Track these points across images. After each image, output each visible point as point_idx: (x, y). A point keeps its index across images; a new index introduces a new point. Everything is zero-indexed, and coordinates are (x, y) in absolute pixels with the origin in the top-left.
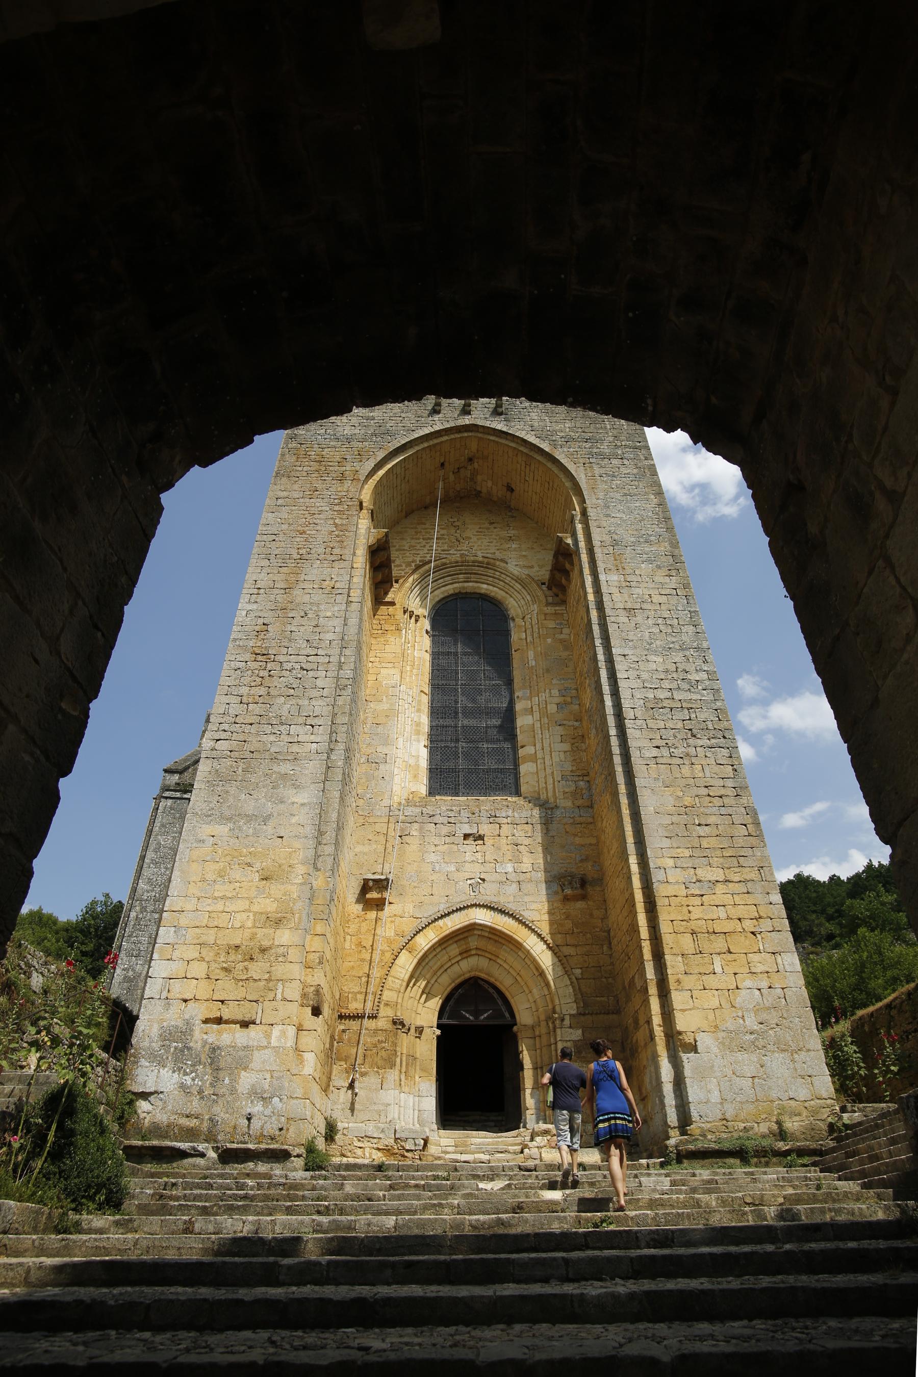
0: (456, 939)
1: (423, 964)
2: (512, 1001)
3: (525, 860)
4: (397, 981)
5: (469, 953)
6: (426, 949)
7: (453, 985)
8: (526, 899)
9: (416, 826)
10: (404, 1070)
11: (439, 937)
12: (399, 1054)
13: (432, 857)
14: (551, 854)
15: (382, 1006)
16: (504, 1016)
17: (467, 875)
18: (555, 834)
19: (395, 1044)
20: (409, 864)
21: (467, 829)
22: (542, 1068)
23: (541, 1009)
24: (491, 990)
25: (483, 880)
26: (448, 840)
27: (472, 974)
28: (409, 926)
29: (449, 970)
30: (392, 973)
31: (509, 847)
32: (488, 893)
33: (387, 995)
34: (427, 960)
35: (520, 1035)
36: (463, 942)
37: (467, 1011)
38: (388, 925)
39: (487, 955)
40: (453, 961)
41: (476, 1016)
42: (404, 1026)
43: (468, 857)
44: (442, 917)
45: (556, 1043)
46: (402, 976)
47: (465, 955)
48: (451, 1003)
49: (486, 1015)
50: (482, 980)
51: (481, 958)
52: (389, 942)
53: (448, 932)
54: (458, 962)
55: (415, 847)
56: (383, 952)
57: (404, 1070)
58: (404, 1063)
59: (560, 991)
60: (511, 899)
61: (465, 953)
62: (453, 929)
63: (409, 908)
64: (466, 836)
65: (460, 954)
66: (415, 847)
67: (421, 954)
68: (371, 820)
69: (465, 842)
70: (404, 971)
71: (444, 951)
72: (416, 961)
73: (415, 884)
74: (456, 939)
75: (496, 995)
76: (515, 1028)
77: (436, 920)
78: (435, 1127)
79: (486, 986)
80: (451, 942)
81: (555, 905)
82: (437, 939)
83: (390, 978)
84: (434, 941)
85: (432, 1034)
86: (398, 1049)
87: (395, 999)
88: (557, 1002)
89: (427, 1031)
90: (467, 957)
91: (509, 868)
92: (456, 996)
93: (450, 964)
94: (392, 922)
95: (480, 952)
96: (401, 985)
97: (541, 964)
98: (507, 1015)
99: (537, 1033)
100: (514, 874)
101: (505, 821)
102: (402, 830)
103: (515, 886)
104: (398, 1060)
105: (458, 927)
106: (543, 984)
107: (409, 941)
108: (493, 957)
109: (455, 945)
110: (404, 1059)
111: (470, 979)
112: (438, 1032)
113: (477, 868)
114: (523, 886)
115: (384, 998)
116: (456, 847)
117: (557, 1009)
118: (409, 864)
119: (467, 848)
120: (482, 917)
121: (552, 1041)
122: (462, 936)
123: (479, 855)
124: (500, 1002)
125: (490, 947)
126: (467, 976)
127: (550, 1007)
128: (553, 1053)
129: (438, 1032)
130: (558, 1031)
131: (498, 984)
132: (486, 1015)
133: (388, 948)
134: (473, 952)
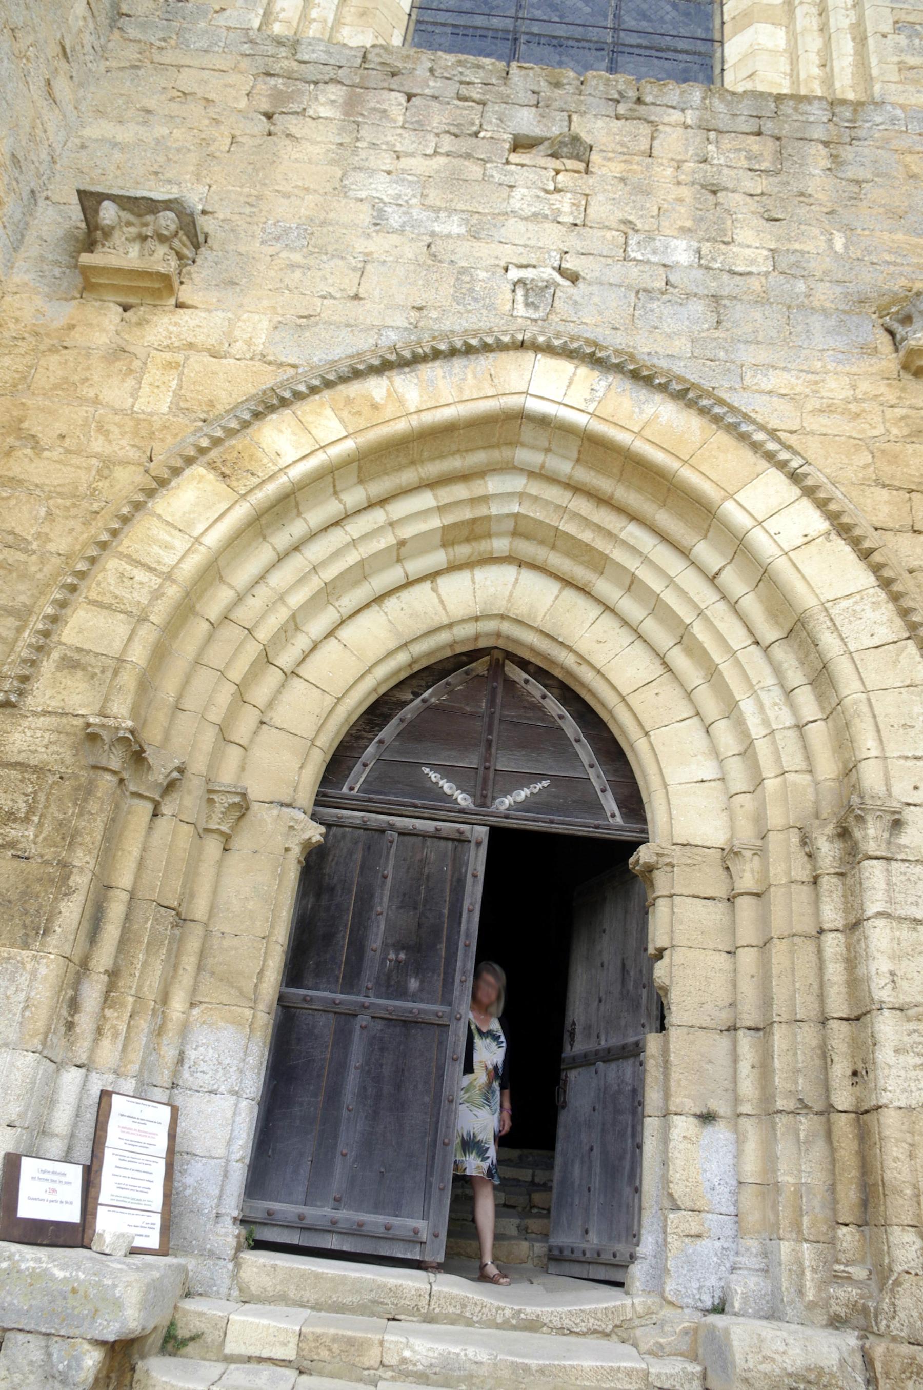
0: (433, 469)
1: (282, 539)
2: (640, 753)
3: (744, 235)
4: (140, 575)
5: (483, 546)
6: (296, 472)
7: (402, 658)
8: (747, 355)
9: (335, 92)
10: (104, 958)
11: (362, 439)
12: (80, 880)
13: (382, 188)
14: (848, 230)
15: (48, 666)
16: (596, 808)
17: (508, 254)
18: (862, 174)
19: (69, 837)
20: (287, 196)
21: (526, 121)
22: (761, 1030)
23: (771, 784)
24: (554, 706)
25: (574, 278)
26: (447, 143)
27: (490, 626)
28: (235, 383)
29: (391, 603)
30: (126, 544)
31: (685, 192)
32: (592, 314)
33: (84, 627)
34: (297, 528)
35: (661, 882)
36: (460, 492)
37: (448, 772)
38: (153, 374)
39: (556, 561)
40: (416, 566)
41: (483, 800)
42: (138, 758)
43: (521, 200)
44: (384, 367)
45: (854, 926)
46: (169, 559)
47: (463, 551)
48: (388, 732)
49: (522, 795)
50: (524, 664)
51: (529, 578)
52: (142, 427)
53: (400, 426)
54: (433, 576)
55: (316, 151)
56: (108, 464)
57: (104, 958)
58: (111, 932)
59: (885, 705)
60: (681, 346)
61: (468, 542)
62: (428, 418)
63: (255, 327)
64: (520, 144)
65: (449, 537)
66: (316, 151)
67: (271, 489)
68: (169, 57)
69: (514, 158)
70: (181, 544)
71: (378, 517)
72: (242, 511)
73: (297, 257)
74: (433, 469)
75: (571, 727)
76: (644, 854)
77: (356, 375)
78: (227, 1235)
79: (536, 689)
80: (409, 476)
81: (864, 386)
82: (349, 445)
83: (112, 564)
84: (335, 452)
85: (285, 832)
86: (83, 859)
87: (116, 648)
88: (867, 744)
89: (265, 818)
90: (469, 565)
91: (681, 252)
92: (409, 712)
93: (395, 575)
94: (170, 365)
95: (527, 549)
96: (157, 595)
97: (800, 588)
98: (610, 804)
99: (747, 881)
100: (698, 274)
101: (675, 116)
102: (278, 97)
103: (697, 308)
104: (71, 912)
105: (448, 413)
106: (795, 676)
107: (231, 433)
108: (580, 573)
109: (426, 500)
110: (116, 909)
111: (474, 655)
112: (316, 832)
113: (552, 237)
114: (738, 311)
115: (69, 635)
116: (474, 170)
117: (871, 776)
118: (287, 196)
119: (521, 176)
120: (554, 388)
121: (831, 914)
122: (455, 463)
123: (565, 204)
124: (585, 752)
125: (577, 518)
126: (465, 631)
127: (827, 767)
128: (835, 971)
129: (316, 832)
130: (874, 872)
131: (587, 675)
132: (522, 795)
133: (133, 454)
134: (500, 545)
